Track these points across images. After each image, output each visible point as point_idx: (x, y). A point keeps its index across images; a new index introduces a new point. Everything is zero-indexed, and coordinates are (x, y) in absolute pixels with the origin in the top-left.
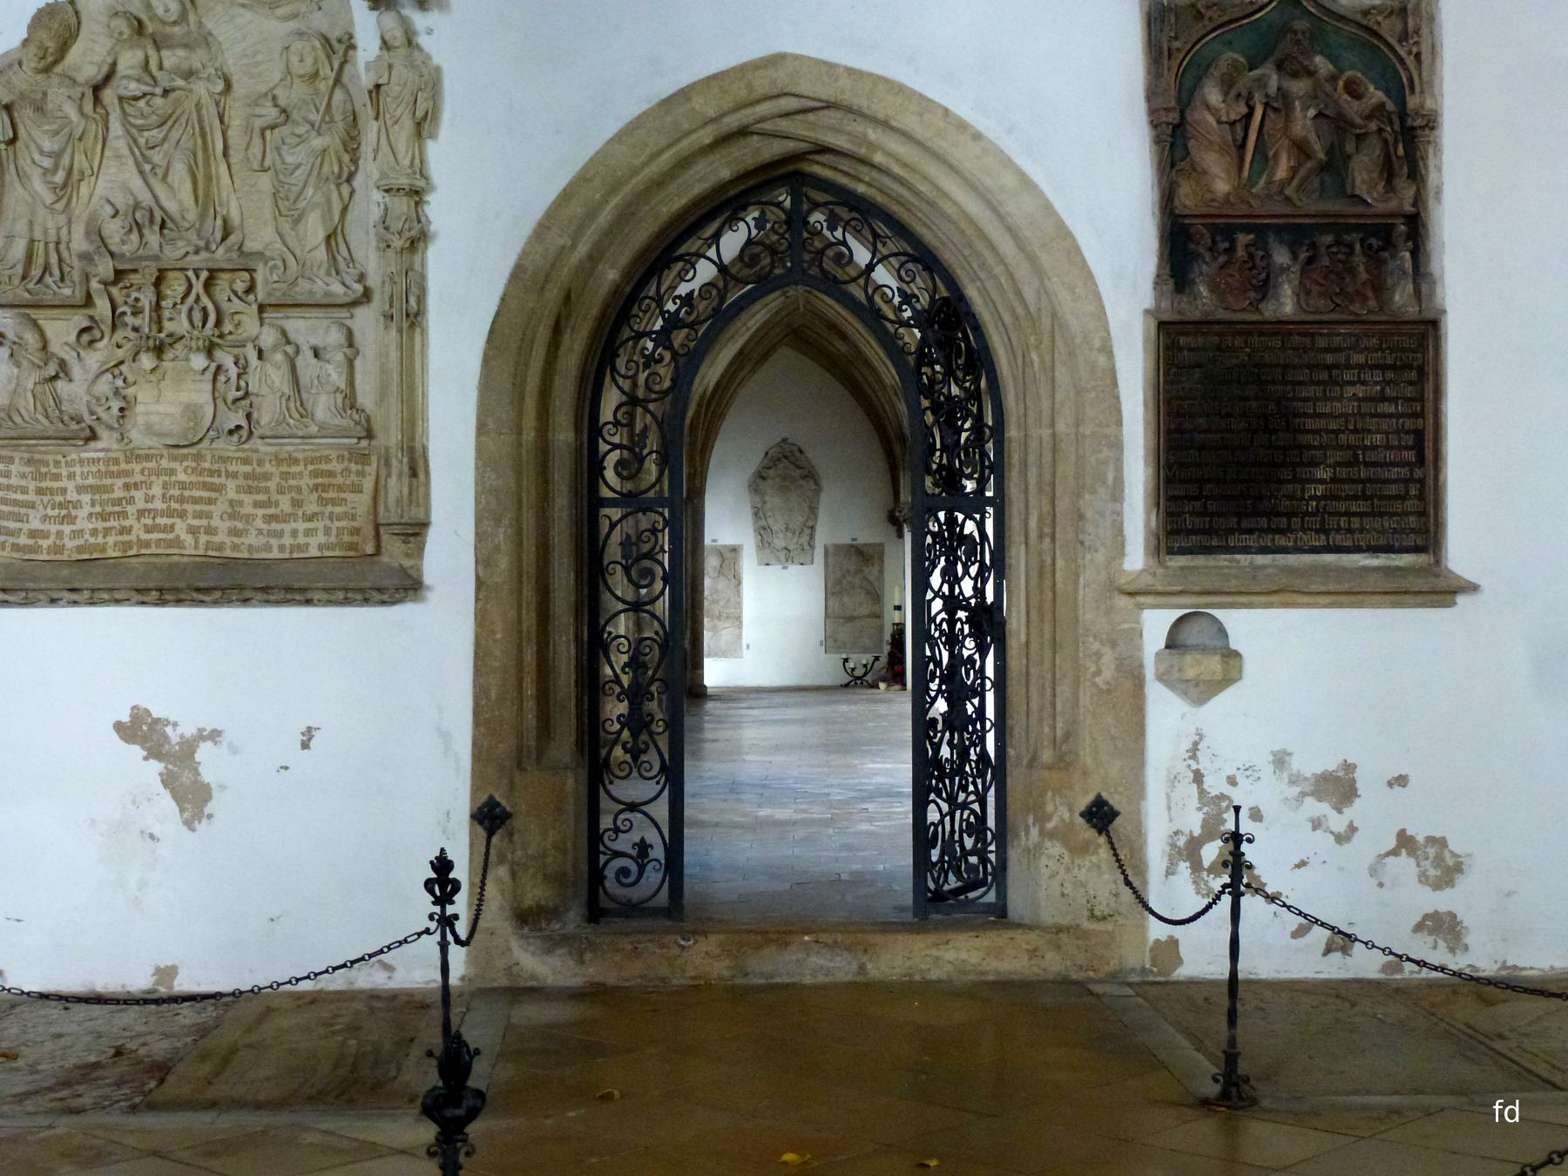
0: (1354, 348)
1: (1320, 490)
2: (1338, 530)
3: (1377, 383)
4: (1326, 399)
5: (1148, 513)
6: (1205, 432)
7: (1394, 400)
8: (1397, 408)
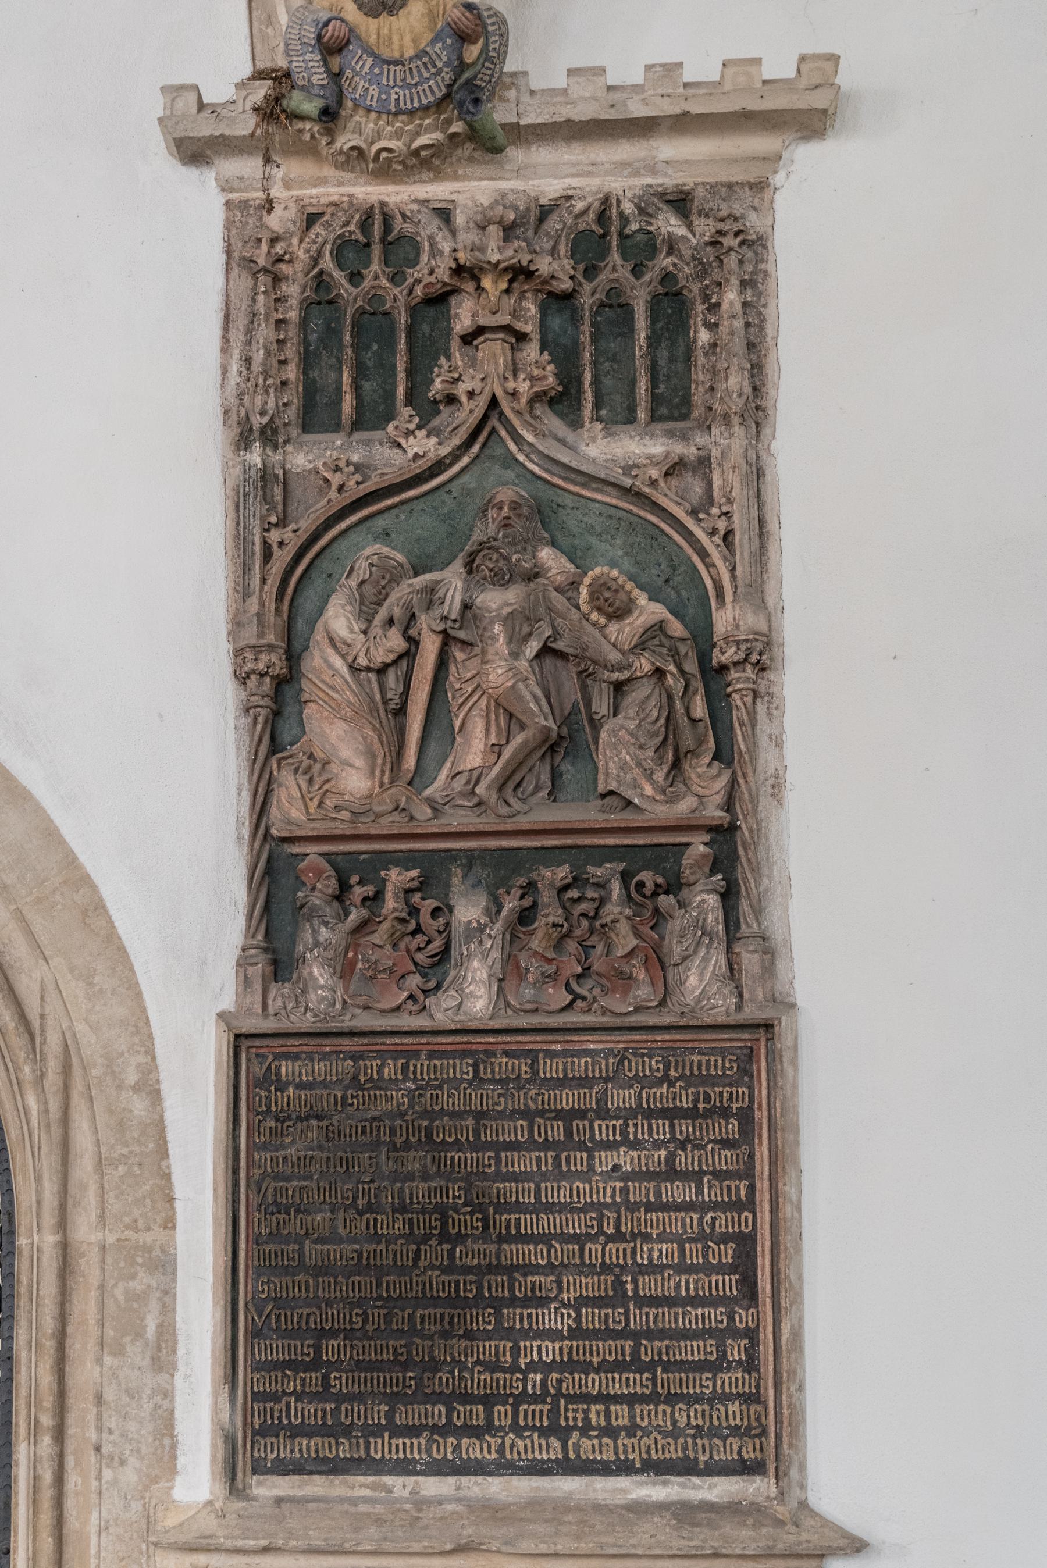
0: (613, 1078)
1: (550, 1351)
2: (586, 1429)
3: (657, 1145)
4: (562, 1176)
5: (216, 1394)
6: (320, 1240)
7: (696, 1176)
8: (699, 1191)
